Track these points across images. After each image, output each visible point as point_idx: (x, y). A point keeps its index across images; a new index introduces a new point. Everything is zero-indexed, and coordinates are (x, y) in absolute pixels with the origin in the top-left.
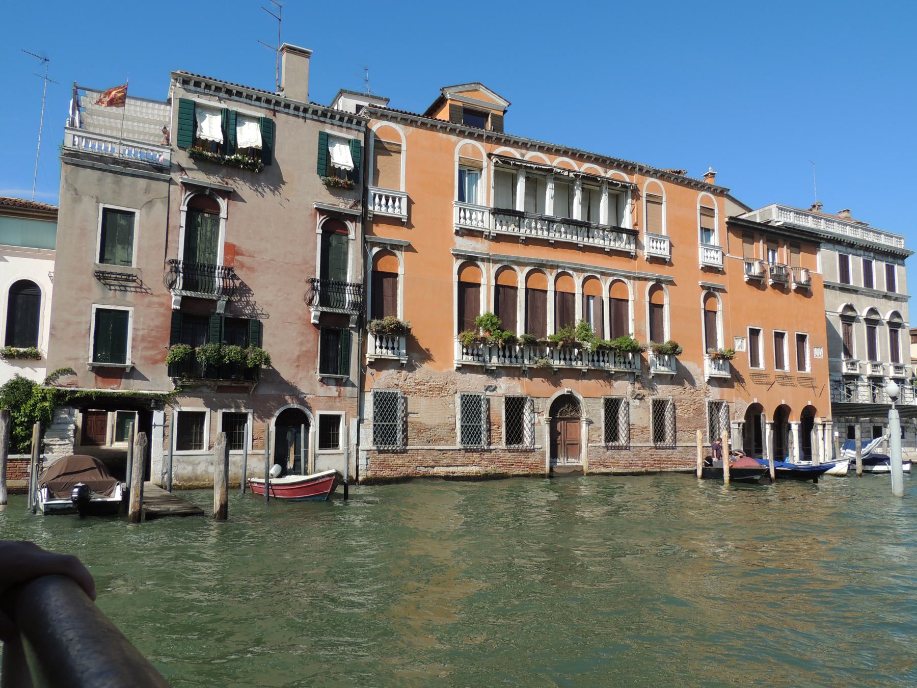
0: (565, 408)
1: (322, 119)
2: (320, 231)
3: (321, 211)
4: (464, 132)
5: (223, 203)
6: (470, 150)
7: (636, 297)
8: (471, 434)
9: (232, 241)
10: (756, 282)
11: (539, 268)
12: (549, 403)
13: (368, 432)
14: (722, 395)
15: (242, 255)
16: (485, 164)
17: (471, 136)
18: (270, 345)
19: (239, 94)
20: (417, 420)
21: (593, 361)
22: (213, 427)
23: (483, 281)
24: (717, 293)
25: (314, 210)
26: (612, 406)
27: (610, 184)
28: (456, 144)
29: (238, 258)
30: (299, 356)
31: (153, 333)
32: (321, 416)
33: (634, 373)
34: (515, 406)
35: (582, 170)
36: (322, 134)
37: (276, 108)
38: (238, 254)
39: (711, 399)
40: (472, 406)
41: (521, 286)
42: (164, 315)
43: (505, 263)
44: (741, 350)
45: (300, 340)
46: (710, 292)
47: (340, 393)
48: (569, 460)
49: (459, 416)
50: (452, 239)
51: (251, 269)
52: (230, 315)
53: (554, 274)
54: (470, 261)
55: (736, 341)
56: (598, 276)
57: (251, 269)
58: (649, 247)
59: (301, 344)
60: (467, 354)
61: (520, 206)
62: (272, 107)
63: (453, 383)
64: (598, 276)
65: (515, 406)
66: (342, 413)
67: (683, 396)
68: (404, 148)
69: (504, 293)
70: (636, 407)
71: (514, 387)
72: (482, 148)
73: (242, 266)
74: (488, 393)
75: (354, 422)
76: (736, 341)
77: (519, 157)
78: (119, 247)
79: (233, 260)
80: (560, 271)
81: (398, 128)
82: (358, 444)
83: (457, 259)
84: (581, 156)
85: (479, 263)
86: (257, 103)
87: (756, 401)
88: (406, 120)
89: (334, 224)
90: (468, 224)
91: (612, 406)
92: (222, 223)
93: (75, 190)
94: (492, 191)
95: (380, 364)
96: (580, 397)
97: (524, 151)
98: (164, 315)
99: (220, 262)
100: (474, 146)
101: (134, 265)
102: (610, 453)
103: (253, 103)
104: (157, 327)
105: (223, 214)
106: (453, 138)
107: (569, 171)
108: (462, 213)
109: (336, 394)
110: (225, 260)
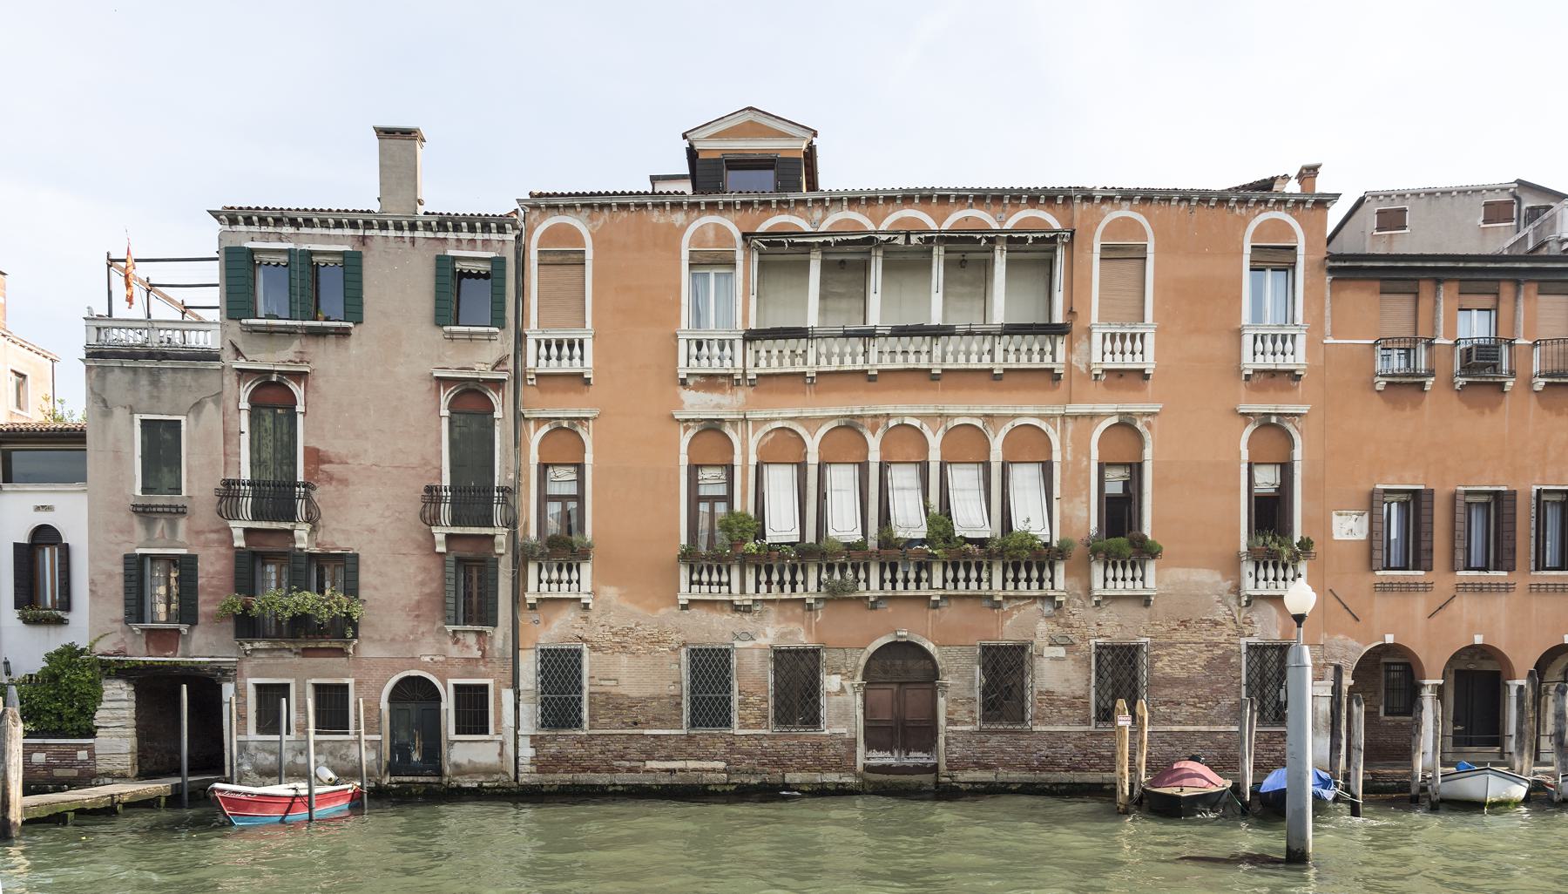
1: (441, 235)
4: (697, 205)
5: (298, 391)
6: (711, 234)
9: (313, 444)
10: (1406, 387)
11: (851, 426)
13: (530, 713)
15: (330, 462)
16: (740, 256)
17: (712, 206)
18: (375, 588)
19: (308, 222)
20: (614, 690)
22: (301, 708)
25: (434, 384)
27: (1010, 240)
28: (683, 229)
30: (419, 602)
31: (215, 582)
32: (456, 686)
35: (946, 226)
36: (443, 263)
37: (368, 233)
38: (324, 462)
42: (226, 557)
45: (419, 578)
47: (484, 652)
49: (686, 683)
50: (677, 395)
51: (344, 482)
52: (316, 550)
53: (880, 432)
54: (712, 427)
56: (979, 423)
57: (344, 482)
58: (1099, 355)
59: (423, 583)
60: (700, 583)
62: (361, 232)
66: (490, 682)
67: (1177, 636)
68: (589, 256)
71: (791, 633)
72: (731, 224)
73: (330, 478)
74: (738, 644)
75: (508, 696)
76: (1336, 520)
77: (807, 228)
78: (165, 470)
79: (317, 470)
80: (892, 423)
82: (517, 727)
83: (686, 429)
84: (944, 199)
85: (728, 430)
86: (338, 232)
87: (1390, 639)
88: (591, 206)
89: (470, 401)
90: (704, 367)
92: (300, 418)
93: (104, 401)
94: (753, 300)
96: (930, 646)
97: (818, 213)
98: (226, 557)
99: (300, 478)
100: (717, 226)
101: (184, 494)
102: (994, 741)
103: (333, 232)
104: (219, 573)
105: (300, 408)
106: (679, 218)
110: (307, 473)
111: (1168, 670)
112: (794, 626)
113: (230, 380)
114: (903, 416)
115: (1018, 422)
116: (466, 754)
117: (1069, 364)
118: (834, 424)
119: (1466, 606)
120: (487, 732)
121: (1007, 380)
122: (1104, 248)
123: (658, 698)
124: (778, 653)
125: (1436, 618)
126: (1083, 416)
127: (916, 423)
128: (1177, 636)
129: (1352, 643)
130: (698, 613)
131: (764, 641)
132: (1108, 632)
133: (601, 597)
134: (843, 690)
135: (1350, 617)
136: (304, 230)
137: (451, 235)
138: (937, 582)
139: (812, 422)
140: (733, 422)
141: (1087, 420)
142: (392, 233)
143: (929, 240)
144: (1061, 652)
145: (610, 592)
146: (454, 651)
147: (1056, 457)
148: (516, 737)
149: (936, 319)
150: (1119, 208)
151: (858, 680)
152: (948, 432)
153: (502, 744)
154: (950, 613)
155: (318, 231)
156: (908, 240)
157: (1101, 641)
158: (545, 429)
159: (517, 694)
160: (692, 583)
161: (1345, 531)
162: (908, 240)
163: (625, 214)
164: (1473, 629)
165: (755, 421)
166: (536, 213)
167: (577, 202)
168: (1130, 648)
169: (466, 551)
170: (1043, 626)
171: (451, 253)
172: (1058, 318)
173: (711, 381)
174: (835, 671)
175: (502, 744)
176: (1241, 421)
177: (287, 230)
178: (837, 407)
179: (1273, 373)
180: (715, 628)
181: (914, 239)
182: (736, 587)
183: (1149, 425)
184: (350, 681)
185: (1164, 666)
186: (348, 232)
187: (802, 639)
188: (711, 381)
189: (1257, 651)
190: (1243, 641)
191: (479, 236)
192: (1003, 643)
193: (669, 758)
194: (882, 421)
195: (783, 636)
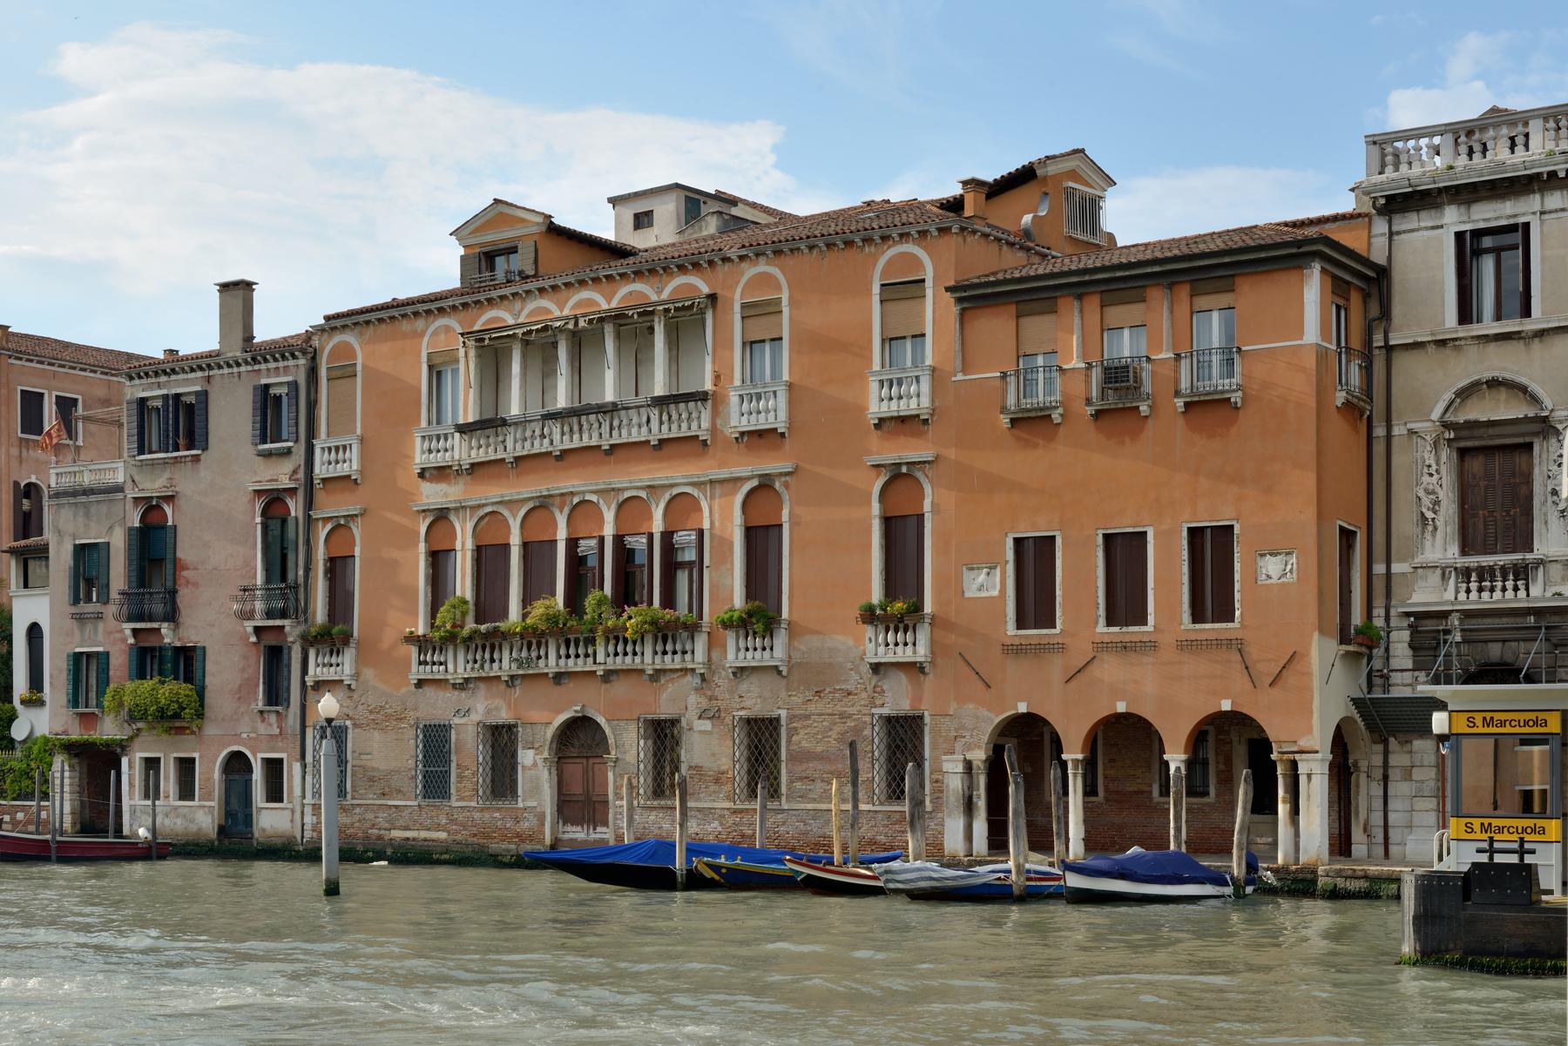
0: (579, 739)
1: (256, 367)
2: (258, 520)
3: (258, 493)
5: (168, 510)
7: (723, 519)
8: (435, 785)
11: (543, 505)
12: (550, 732)
14: (917, 698)
21: (616, 654)
23: (458, 546)
24: (919, 475)
26: (664, 734)
29: (185, 573)
33: (693, 670)
34: (502, 740)
39: (886, 711)
40: (436, 741)
41: (515, 540)
43: (489, 509)
44: (983, 594)
46: (899, 477)
48: (599, 829)
51: (196, 585)
52: (178, 644)
53: (566, 510)
54: (441, 516)
55: (967, 576)
56: (643, 494)
57: (196, 585)
58: (737, 419)
59: (243, 670)
60: (426, 663)
61: (515, 410)
63: (416, 709)
65: (502, 740)
67: (812, 708)
69: (489, 558)
70: (700, 732)
71: (497, 709)
74: (456, 720)
75: (297, 767)
76: (967, 576)
80: (576, 500)
82: (304, 797)
87: (1022, 708)
91: (664, 734)
95: (320, 686)
96: (601, 720)
107: (576, 318)
108: (426, 444)
109: (277, 731)
111: (804, 744)
112: (498, 702)
113: (129, 505)
114: (584, 493)
115: (676, 491)
116: (270, 820)
117: (714, 429)
118: (530, 505)
119: (1110, 670)
120: (281, 800)
121: (666, 450)
122: (744, 306)
123: (398, 772)
125: (1073, 683)
126: (722, 482)
127: (594, 498)
128: (812, 708)
129: (984, 712)
130: (429, 691)
131: (475, 718)
132: (748, 703)
133: (362, 678)
134: (535, 764)
135: (980, 685)
136: (173, 377)
137: (263, 366)
138: (600, 657)
139: (511, 504)
140: (456, 509)
141: (731, 485)
142: (226, 371)
143: (601, 320)
144: (706, 725)
145: (368, 673)
146: (262, 729)
147: (706, 525)
148: (303, 806)
149: (609, 396)
150: (757, 264)
151: (546, 755)
152: (621, 506)
153: (293, 811)
154: (620, 688)
155: (181, 376)
156: (576, 324)
157: (742, 713)
158: (329, 527)
159: (304, 766)
160: (420, 663)
161: (975, 587)
162: (576, 324)
163: (383, 326)
165: (472, 508)
166: (326, 335)
167: (348, 321)
169: (271, 640)
170: (693, 699)
171: (264, 381)
172: (708, 386)
173: (440, 473)
174: (530, 746)
175: (293, 811)
176: (873, 473)
177: (163, 379)
178: (530, 487)
180: (437, 706)
181: (582, 323)
182: (451, 667)
183: (786, 485)
184: (196, 755)
185: (803, 740)
186: (199, 374)
187: (504, 716)
188: (440, 473)
189: (892, 722)
191: (281, 364)
192: (663, 717)
193: (407, 828)
194: (568, 499)
195: (488, 712)
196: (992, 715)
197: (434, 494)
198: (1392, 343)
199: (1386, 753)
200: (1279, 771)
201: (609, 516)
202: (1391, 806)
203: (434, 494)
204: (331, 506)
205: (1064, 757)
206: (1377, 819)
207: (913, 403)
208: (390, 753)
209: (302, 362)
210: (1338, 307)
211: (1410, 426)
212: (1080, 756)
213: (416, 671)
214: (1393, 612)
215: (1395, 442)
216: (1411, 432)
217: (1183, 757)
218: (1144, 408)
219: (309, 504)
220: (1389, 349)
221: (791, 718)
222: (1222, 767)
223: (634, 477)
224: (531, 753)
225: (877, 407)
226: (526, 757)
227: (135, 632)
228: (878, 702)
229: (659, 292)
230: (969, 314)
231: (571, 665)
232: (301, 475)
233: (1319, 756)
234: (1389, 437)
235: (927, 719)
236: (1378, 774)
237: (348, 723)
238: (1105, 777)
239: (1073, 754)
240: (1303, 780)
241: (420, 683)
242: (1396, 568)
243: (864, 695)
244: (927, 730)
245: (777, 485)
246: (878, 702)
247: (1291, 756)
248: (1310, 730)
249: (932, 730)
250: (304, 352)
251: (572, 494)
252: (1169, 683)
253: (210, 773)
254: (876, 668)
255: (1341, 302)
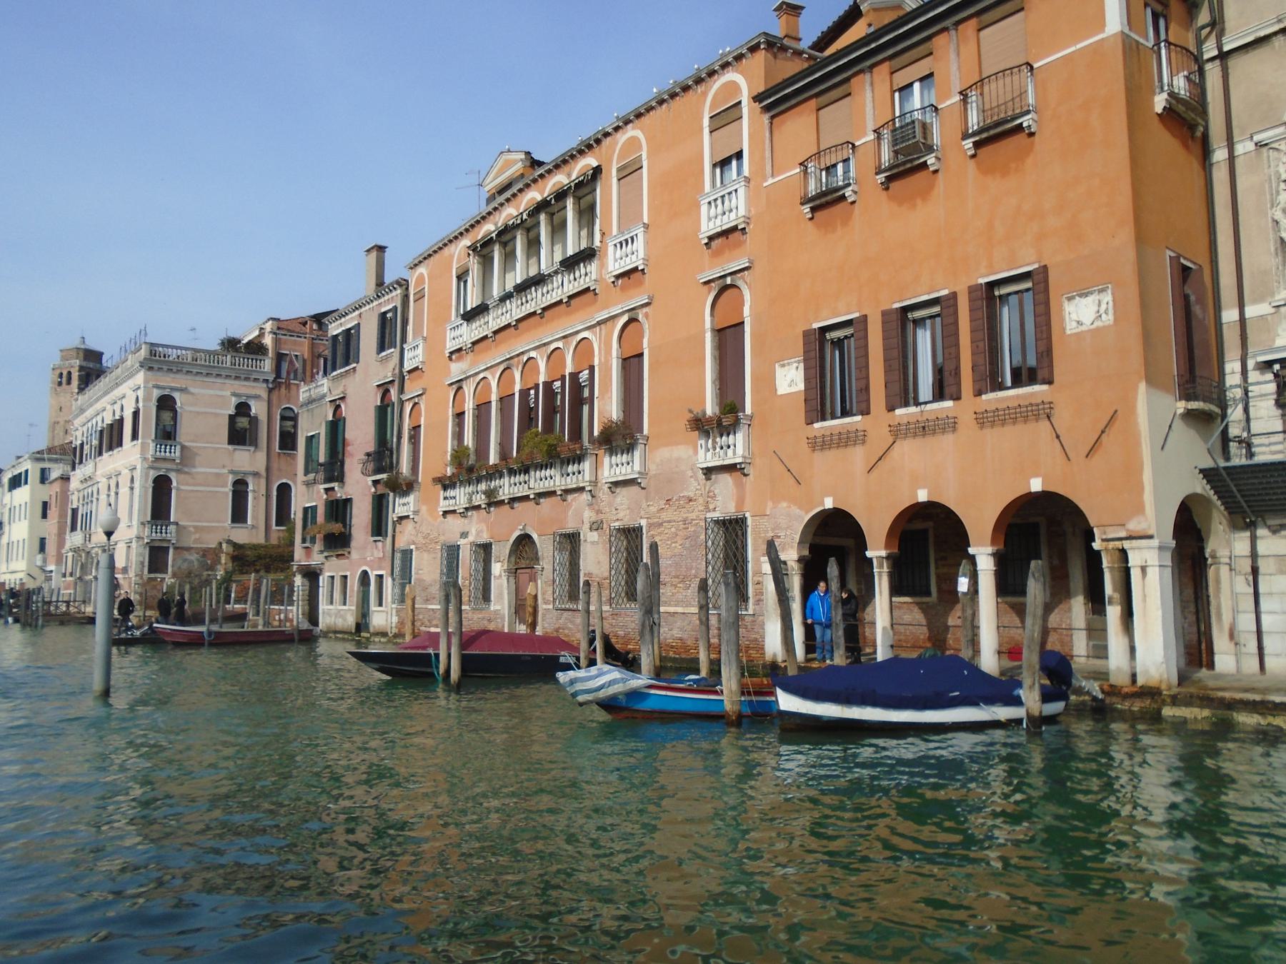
14: (740, 502)
24: (740, 283)
28: (452, 256)
33: (582, 489)
39: (716, 515)
43: (481, 376)
44: (794, 389)
54: (458, 385)
56: (560, 344)
58: (615, 261)
64: (560, 344)
67: (665, 516)
70: (593, 543)
75: (390, 579)
76: (780, 372)
81: (422, 270)
87: (829, 504)
95: (401, 518)
96: (535, 536)
122: (619, 170)
124: (479, 546)
125: (875, 471)
129: (795, 510)
131: (471, 538)
132: (621, 515)
144: (594, 536)
147: (596, 362)
157: (617, 524)
164: (916, 484)
168: (634, 529)
178: (497, 355)
179: (725, 233)
183: (646, 315)
186: (357, 312)
187: (485, 538)
190: (709, 515)
195: (478, 533)
196: (802, 513)
197: (457, 369)
198: (1226, 49)
199: (1253, 540)
200: (1105, 564)
201: (542, 365)
202: (1264, 605)
203: (457, 369)
204: (412, 390)
205: (869, 554)
206: (1246, 622)
207: (733, 216)
208: (427, 569)
209: (399, 291)
210: (1156, 17)
211: (1256, 138)
212: (883, 553)
213: (444, 505)
214: (1251, 364)
215: (1239, 164)
216: (1260, 145)
217: (990, 550)
218: (931, 160)
219: (401, 391)
220: (1223, 56)
221: (650, 526)
222: (1056, 562)
223: (551, 332)
224: (499, 565)
225: (708, 226)
226: (497, 568)
227: (327, 490)
228: (711, 507)
229: (569, 175)
230: (775, 120)
231: (520, 491)
232: (397, 371)
233: (1155, 543)
234: (1232, 158)
235: (749, 522)
236: (1246, 566)
237: (412, 547)
238: (938, 576)
239: (876, 551)
240: (1135, 575)
241: (445, 513)
242: (1250, 311)
243: (701, 500)
244: (749, 530)
245: (640, 317)
246: (711, 507)
247: (1118, 544)
248: (1139, 509)
249: (753, 530)
250: (401, 286)
251: (522, 353)
252: (971, 465)
253: (354, 585)
254: (708, 472)
255: (1159, 8)
